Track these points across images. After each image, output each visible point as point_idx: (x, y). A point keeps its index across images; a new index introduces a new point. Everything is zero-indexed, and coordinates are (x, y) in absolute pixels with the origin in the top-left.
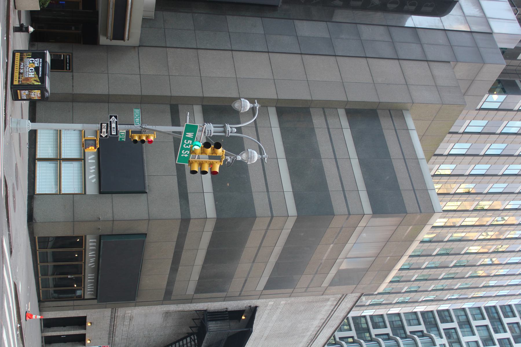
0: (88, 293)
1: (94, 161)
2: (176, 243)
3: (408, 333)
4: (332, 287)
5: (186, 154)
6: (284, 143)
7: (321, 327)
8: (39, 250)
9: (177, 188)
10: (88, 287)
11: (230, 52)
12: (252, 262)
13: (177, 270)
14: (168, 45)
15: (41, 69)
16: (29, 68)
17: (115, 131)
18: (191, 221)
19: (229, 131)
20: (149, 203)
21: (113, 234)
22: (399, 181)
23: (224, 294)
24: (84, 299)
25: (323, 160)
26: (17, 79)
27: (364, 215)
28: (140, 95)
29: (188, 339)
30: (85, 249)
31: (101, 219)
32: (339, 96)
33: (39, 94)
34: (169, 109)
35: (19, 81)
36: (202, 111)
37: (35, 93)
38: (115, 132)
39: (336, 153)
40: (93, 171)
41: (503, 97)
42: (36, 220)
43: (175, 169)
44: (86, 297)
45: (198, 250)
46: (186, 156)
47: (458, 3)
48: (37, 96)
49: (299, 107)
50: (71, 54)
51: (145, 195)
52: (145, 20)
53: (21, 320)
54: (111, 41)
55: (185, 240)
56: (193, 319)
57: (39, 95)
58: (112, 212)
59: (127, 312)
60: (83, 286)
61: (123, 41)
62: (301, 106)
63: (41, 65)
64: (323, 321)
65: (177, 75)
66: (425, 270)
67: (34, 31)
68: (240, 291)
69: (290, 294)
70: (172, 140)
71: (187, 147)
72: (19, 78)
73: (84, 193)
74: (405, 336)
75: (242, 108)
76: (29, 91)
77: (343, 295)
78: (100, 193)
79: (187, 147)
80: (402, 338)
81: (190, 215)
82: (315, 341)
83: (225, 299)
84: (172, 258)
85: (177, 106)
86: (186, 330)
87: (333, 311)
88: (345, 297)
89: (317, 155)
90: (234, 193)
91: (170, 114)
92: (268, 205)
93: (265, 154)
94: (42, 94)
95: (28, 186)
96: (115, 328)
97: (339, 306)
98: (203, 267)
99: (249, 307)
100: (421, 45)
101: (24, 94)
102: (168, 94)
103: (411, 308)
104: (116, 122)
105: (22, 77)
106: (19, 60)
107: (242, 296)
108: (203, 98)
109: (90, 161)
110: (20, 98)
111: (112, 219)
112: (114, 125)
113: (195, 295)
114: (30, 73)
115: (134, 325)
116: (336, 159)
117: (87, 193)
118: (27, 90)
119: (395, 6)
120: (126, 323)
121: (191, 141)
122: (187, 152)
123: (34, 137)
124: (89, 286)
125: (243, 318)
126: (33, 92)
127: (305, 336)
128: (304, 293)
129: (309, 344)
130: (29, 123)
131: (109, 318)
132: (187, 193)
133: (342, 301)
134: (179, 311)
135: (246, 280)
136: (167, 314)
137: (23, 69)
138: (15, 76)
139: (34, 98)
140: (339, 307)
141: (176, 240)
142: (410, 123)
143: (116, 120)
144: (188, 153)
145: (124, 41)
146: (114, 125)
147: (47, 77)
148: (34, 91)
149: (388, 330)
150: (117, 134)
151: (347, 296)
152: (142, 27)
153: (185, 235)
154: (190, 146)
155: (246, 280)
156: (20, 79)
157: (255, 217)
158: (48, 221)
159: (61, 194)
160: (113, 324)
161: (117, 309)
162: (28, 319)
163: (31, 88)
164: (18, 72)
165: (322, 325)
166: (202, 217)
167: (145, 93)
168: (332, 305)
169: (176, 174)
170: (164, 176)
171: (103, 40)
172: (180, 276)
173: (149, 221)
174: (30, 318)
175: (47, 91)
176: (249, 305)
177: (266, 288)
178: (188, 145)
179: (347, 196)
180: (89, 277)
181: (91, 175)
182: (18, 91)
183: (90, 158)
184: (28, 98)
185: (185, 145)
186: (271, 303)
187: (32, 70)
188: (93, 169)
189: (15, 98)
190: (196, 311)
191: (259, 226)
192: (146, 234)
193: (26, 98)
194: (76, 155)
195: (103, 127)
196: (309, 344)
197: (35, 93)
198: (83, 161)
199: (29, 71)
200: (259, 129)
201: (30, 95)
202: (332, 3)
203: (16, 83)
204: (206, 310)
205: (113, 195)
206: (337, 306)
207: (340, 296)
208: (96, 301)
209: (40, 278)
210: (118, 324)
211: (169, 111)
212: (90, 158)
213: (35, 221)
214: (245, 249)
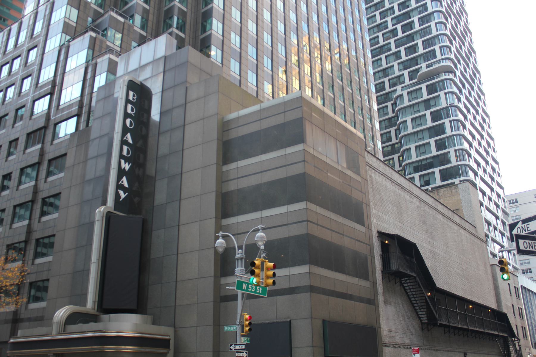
3: (394, 115)
4: (361, 173)
5: (259, 289)
6: (250, 212)
7: (392, 181)
11: (179, 255)
14: (174, 305)
18: (311, 284)
22: (278, 124)
23: (369, 257)
25: (262, 182)
27: (304, 150)
29: (405, 285)
32: (213, 170)
34: (224, 303)
39: (257, 172)
41: (213, 48)
43: (271, 298)
51: (292, 321)
52: (154, 323)
56: (389, 281)
59: (385, 334)
62: (221, 200)
64: (387, 180)
65: (197, 297)
70: (248, 300)
71: (254, 288)
74: (400, 144)
77: (367, 165)
79: (254, 288)
80: (398, 120)
82: (404, 186)
83: (373, 256)
86: (398, 287)
87: (380, 172)
89: (258, 187)
92: (299, 224)
96: (398, 344)
98: (348, 274)
102: (212, 304)
103: (379, 153)
104: (235, 345)
108: (215, 276)
112: (237, 347)
113: (370, 281)
115: (395, 329)
116: (261, 172)
119: (144, 129)
120: (394, 335)
121: (250, 285)
125: (387, 242)
127: (399, 194)
129: (406, 190)
131: (390, 348)
134: (383, 293)
135: (358, 240)
136: (386, 302)
140: (376, 168)
141: (327, 296)
142: (233, 116)
143: (233, 345)
146: (237, 347)
149: (392, 130)
150: (245, 344)
151: (368, 162)
152: (160, 325)
154: (253, 286)
155: (358, 240)
160: (395, 345)
161: (383, 342)
165: (391, 180)
167: (211, 322)
168: (375, 173)
169: (275, 297)
177: (363, 224)
178: (252, 288)
179: (290, 163)
186: (375, 220)
190: (383, 279)
191: (315, 231)
192: (323, 320)
196: (406, 190)
204: (382, 272)
207: (367, 167)
210: (394, 341)
211: (225, 303)
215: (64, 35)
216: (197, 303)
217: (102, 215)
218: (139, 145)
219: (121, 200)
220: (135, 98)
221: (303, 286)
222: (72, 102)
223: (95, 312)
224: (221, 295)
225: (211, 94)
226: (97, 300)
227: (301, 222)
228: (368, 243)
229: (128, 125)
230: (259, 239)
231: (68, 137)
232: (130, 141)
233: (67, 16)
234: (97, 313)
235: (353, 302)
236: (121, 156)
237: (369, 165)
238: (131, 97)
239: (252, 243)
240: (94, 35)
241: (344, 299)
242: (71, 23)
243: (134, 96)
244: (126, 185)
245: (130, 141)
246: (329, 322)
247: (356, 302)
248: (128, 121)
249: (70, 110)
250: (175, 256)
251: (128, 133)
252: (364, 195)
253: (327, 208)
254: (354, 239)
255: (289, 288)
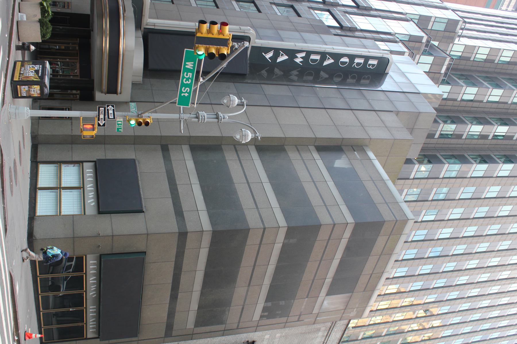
0: (91, 330)
1: (93, 189)
2: (175, 264)
5: (186, 92)
8: (44, 327)
9: (173, 208)
10: (91, 323)
11: (210, 105)
12: (247, 285)
13: (176, 298)
14: (156, 101)
15: (40, 71)
16: (30, 70)
17: (113, 116)
18: (189, 234)
19: (221, 117)
20: (147, 220)
21: (113, 252)
23: (221, 327)
24: (86, 339)
26: (18, 77)
27: (348, 223)
28: (133, 136)
30: (86, 274)
31: (101, 235)
32: (308, 134)
33: (39, 90)
35: (19, 79)
36: (189, 149)
37: (34, 89)
38: (113, 116)
39: (314, 178)
40: (92, 196)
41: (430, 166)
42: (36, 237)
43: (170, 192)
44: (89, 336)
45: (196, 271)
46: (186, 96)
47: (388, 74)
48: (37, 92)
49: (274, 144)
50: (69, 107)
51: (142, 213)
52: (134, 84)
53: (19, 331)
54: (105, 94)
55: (183, 258)
57: (39, 92)
58: (111, 228)
60: (85, 322)
61: (116, 95)
62: (276, 144)
63: (41, 69)
66: (385, 337)
67: (35, 50)
68: (237, 322)
69: (284, 324)
70: (165, 171)
71: (187, 82)
72: (19, 76)
73: (83, 214)
75: (231, 102)
76: (29, 86)
78: (100, 212)
79: (187, 82)
81: (187, 229)
84: (171, 282)
85: (167, 145)
88: (334, 325)
90: (226, 210)
91: (161, 152)
93: (258, 134)
94: (42, 90)
95: (29, 210)
97: (329, 336)
98: (202, 294)
99: (247, 343)
100: (368, 101)
101: (23, 90)
104: (113, 110)
105: (22, 76)
106: (20, 66)
107: (239, 329)
108: (190, 137)
109: (88, 189)
110: (19, 96)
111: (112, 235)
112: (111, 112)
113: (195, 329)
114: (30, 74)
116: (314, 182)
117: (86, 214)
118: (27, 85)
119: (340, 79)
121: (191, 74)
122: (187, 90)
123: (35, 171)
124: (91, 280)
126: (33, 87)
128: (297, 322)
130: (27, 109)
132: (182, 211)
133: (332, 331)
135: (243, 309)
137: (24, 71)
138: (15, 75)
139: (34, 95)
140: (329, 338)
141: (174, 260)
142: (371, 155)
143: (113, 108)
144: (188, 91)
145: (117, 95)
146: (111, 112)
147: (46, 77)
148: (33, 87)
150: (114, 118)
151: (336, 325)
152: (132, 89)
153: (183, 252)
154: (190, 80)
155: (243, 309)
156: (20, 77)
157: (249, 230)
158: (48, 238)
159: (61, 215)
162: (27, 338)
163: (30, 83)
164: (19, 73)
166: (199, 230)
169: (170, 196)
170: (159, 199)
171: (99, 96)
172: (180, 306)
173: (148, 235)
174: (30, 338)
175: (46, 87)
176: (247, 340)
177: (262, 317)
178: (187, 79)
179: (329, 209)
180: (91, 310)
181: (90, 200)
182: (18, 86)
183: (88, 186)
184: (28, 95)
185: (185, 79)
186: (267, 336)
187: (33, 72)
188: (92, 195)
189: (15, 95)
191: (252, 241)
192: (145, 252)
193: (26, 95)
194: (76, 185)
195: (100, 112)
197: (34, 88)
198: (82, 189)
199: (29, 72)
200: (242, 161)
201: (29, 92)
202: (289, 77)
203: (16, 79)
205: (111, 214)
206: (328, 337)
207: (329, 324)
208: (99, 339)
209: (41, 313)
211: (161, 149)
212: (88, 186)
213: (35, 238)
214: (240, 269)
215: (417, 17)
216: (158, 121)
217: (246, 31)
218: (323, 75)
219: (263, 53)
220: (371, 67)
221: (185, 225)
222: (353, 22)
223: (144, 26)
224: (169, 146)
225: (390, 132)
226: (156, 28)
227: (262, 221)
228: (241, 325)
229: (343, 60)
230: (243, 133)
231: (318, 18)
232: (326, 63)
233: (437, 20)
234: (142, 28)
235: (168, 302)
236: (309, 53)
237: (333, 326)
238: (371, 62)
239: (231, 174)
240: (424, 41)
241: (172, 286)
242: (431, 24)
243: (373, 65)
244: (279, 60)
245: (326, 63)
246: (144, 259)
247: (168, 305)
248: (345, 60)
249: (345, 21)
250: (209, 102)
251: (334, 60)
252: (296, 318)
253: (280, 259)
254: (244, 302)
255: (182, 210)
